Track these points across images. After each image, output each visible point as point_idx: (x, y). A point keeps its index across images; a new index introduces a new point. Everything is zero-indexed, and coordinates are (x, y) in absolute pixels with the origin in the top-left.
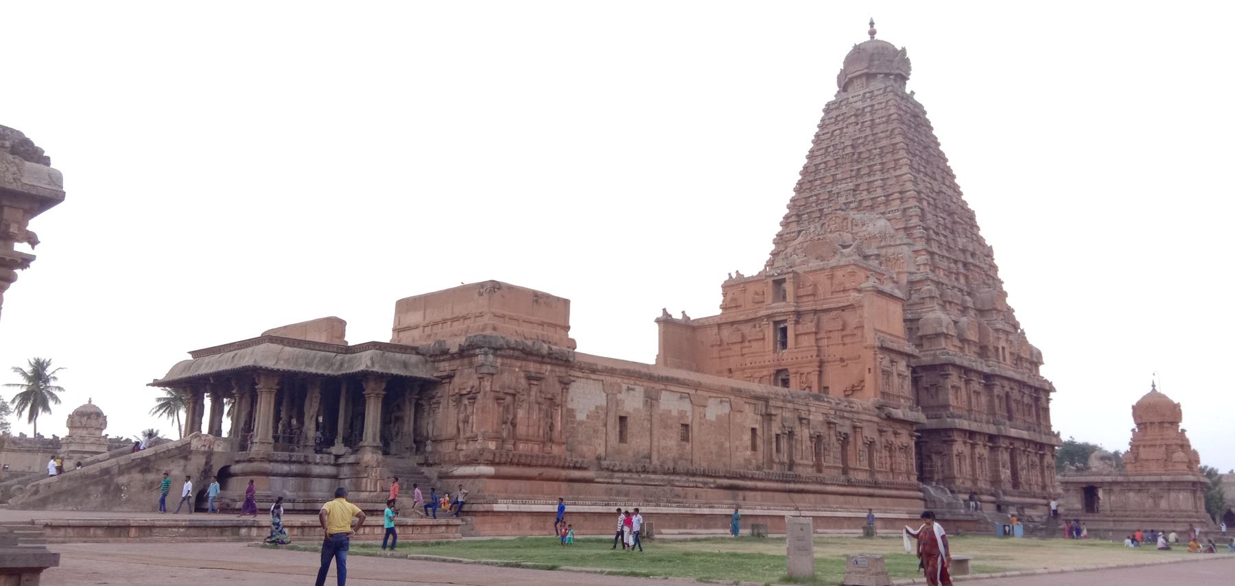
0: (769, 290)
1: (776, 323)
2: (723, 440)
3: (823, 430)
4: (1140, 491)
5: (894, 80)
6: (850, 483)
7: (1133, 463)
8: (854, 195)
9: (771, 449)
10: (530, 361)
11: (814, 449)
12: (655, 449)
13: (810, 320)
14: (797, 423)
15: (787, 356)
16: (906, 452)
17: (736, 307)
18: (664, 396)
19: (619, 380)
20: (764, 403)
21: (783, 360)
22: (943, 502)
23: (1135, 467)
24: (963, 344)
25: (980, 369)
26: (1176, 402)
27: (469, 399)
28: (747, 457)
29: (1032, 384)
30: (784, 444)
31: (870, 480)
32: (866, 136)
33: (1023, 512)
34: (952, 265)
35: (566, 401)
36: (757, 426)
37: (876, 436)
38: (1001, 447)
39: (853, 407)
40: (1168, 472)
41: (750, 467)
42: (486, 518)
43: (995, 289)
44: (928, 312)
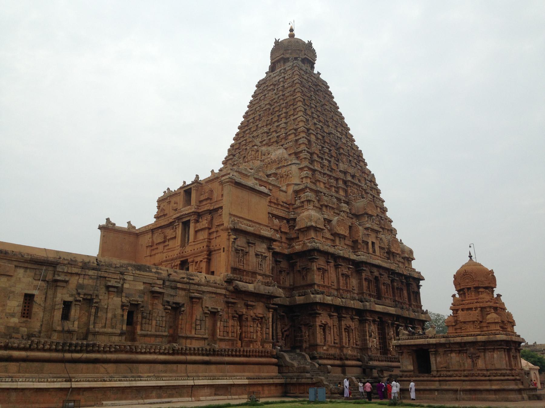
0: (180, 199)
4: (460, 352)
6: (175, 352)
7: (452, 326)
11: (125, 317)
13: (205, 218)
14: (103, 290)
15: (189, 249)
20: (51, 268)
21: (186, 252)
23: (456, 329)
24: (334, 237)
25: (347, 256)
26: (490, 269)
28: (12, 325)
29: (401, 272)
32: (278, 97)
36: (36, 292)
38: (368, 320)
39: (193, 280)
40: (482, 333)
41: (14, 335)
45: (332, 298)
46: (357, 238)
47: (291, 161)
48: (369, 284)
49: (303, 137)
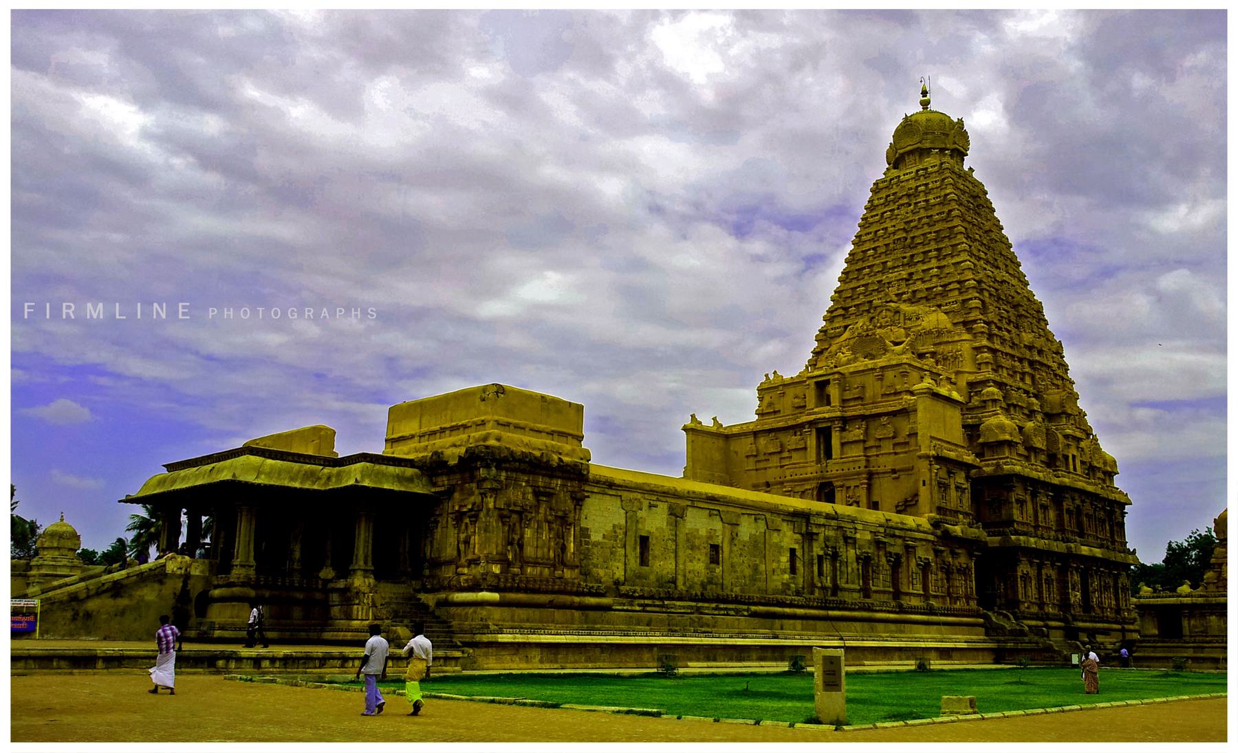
0: (811, 394)
1: (819, 431)
2: (758, 562)
3: (871, 550)
5: (950, 155)
6: (902, 610)
7: (1214, 583)
8: (907, 285)
9: (812, 572)
10: (538, 474)
12: (680, 572)
14: (842, 542)
16: (965, 574)
17: (775, 412)
18: (690, 513)
19: (639, 496)
20: (804, 520)
22: (1006, 628)
27: (470, 517)
28: (785, 581)
30: (827, 567)
31: (924, 605)
32: (920, 219)
33: (1095, 638)
34: (1017, 364)
35: (579, 520)
36: (796, 546)
37: (931, 557)
38: (1072, 567)
39: (905, 524)
41: (789, 592)
42: (490, 650)
43: (1064, 390)
44: (990, 416)
45: (1036, 539)
46: (1054, 451)
47: (959, 335)
48: (1070, 517)
49: (975, 298)
